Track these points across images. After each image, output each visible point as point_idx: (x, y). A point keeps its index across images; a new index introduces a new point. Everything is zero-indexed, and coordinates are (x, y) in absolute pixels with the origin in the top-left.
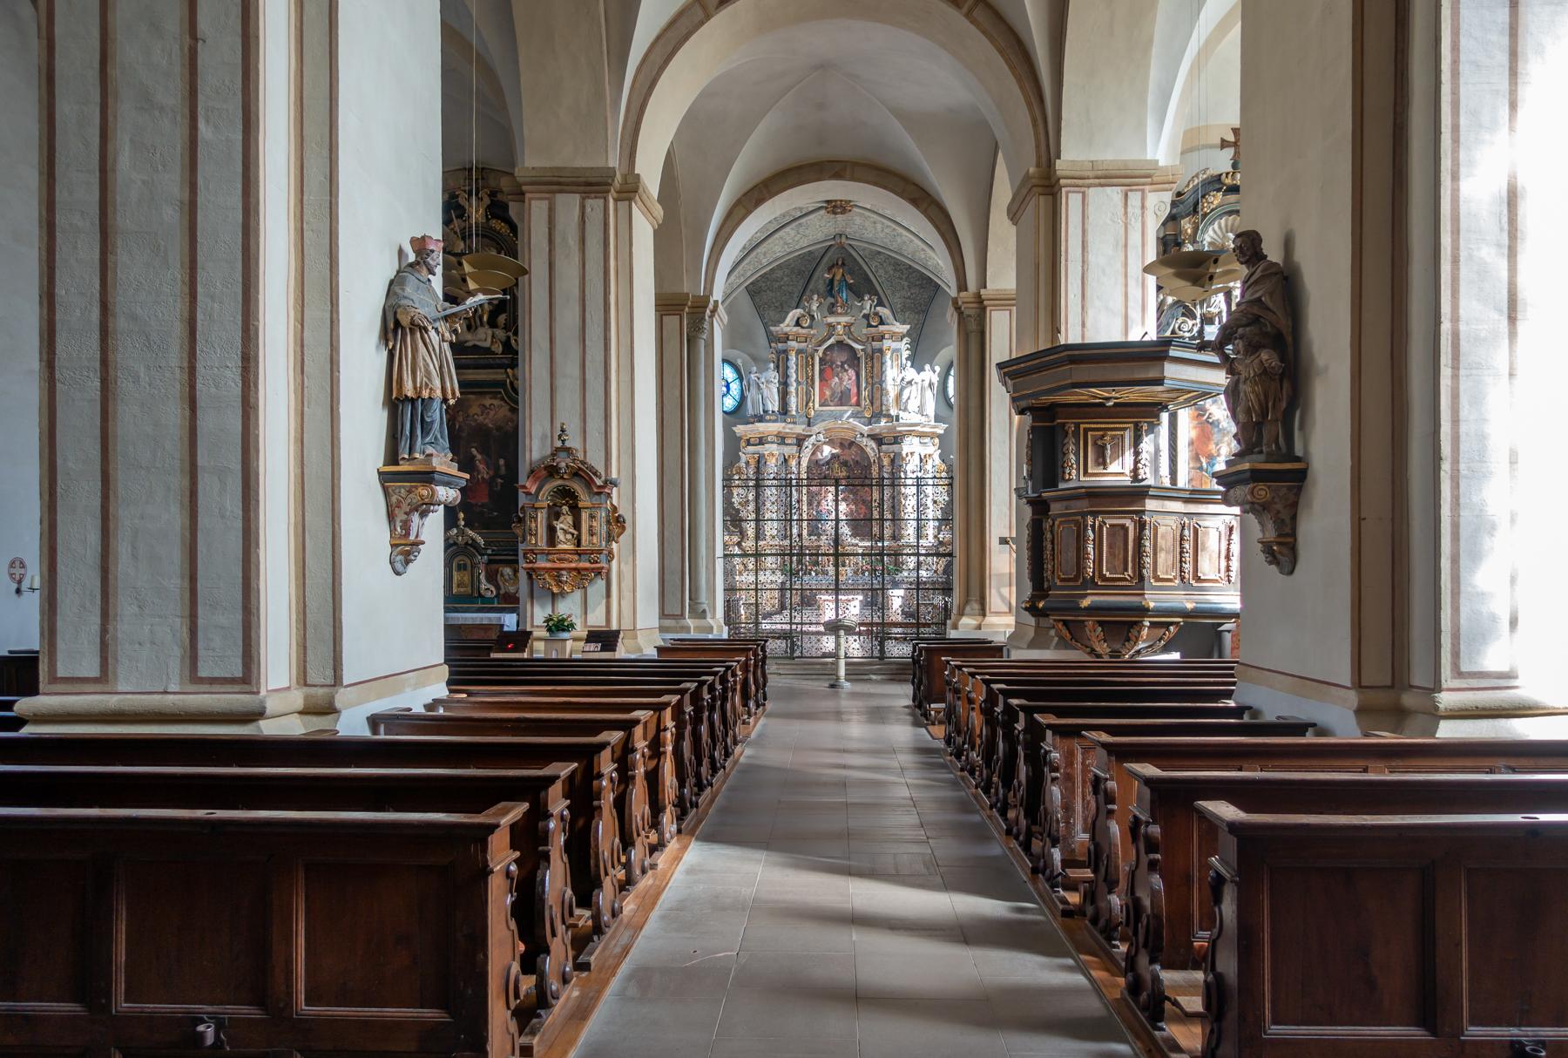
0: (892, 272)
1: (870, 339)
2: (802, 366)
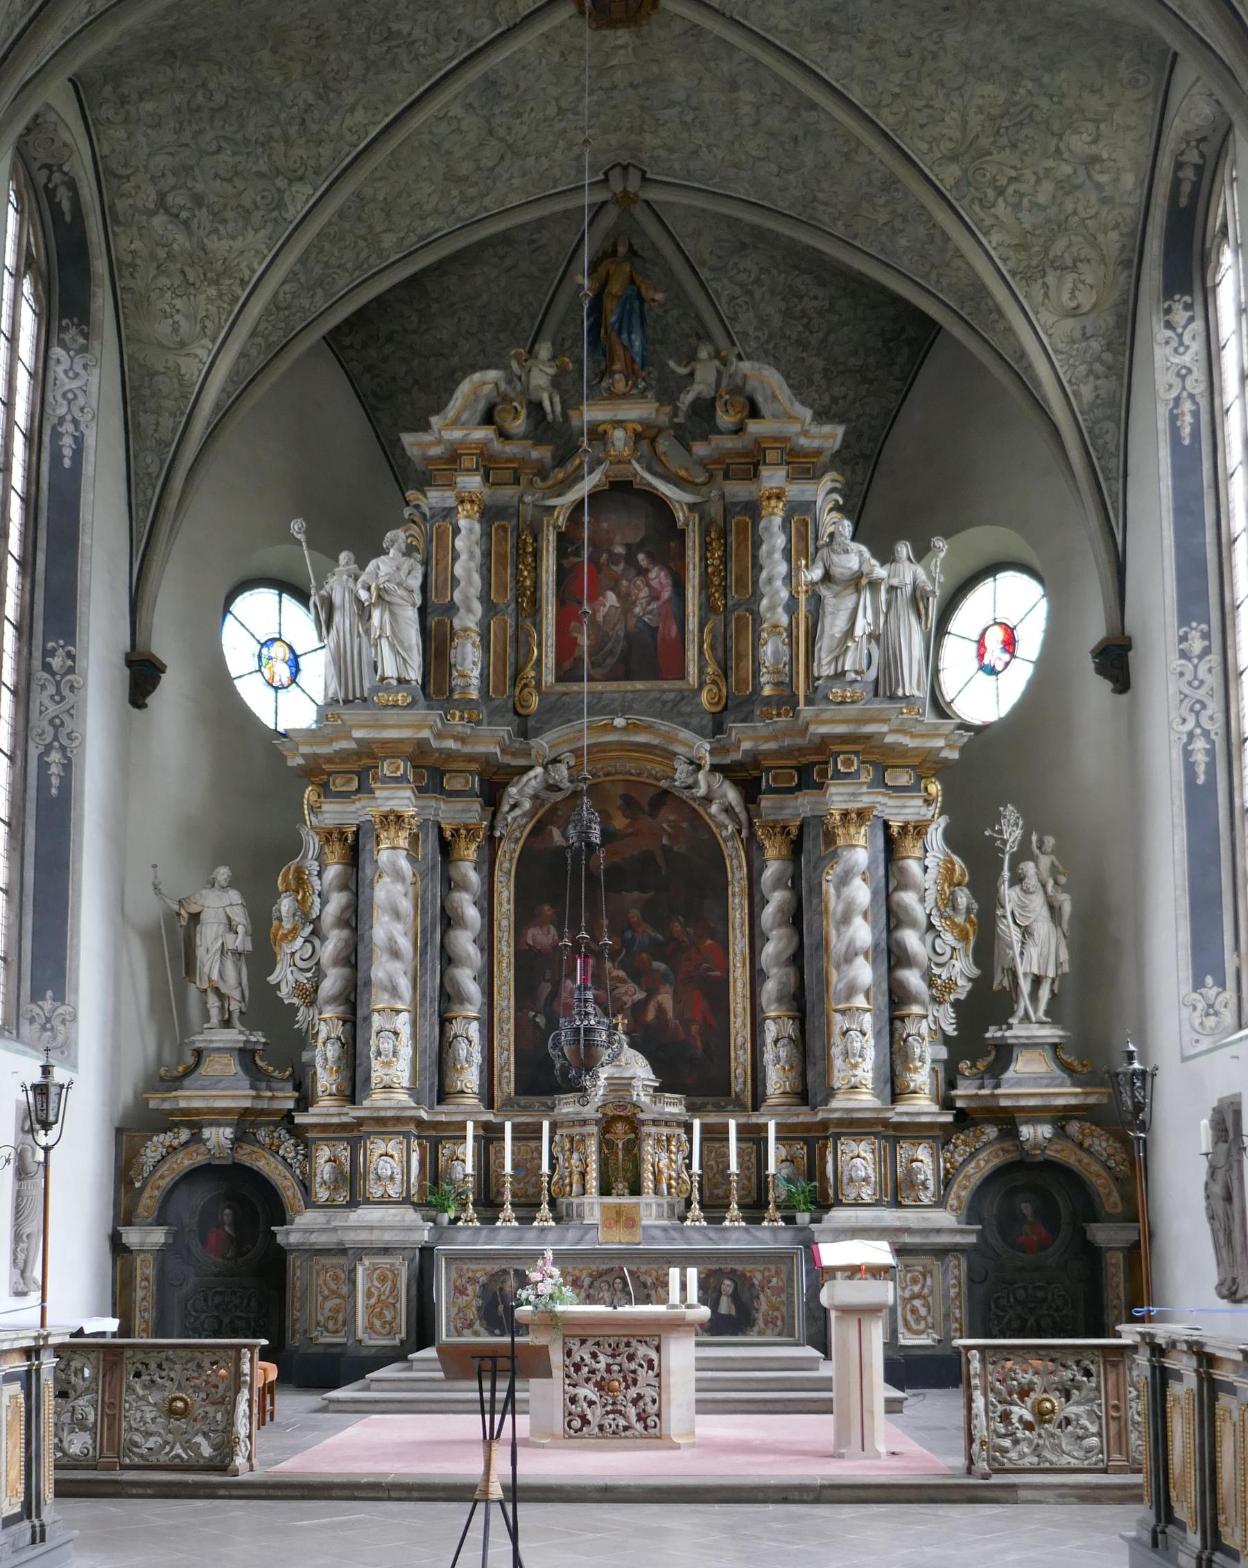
0: (777, 321)
1: (720, 475)
2: (502, 558)
